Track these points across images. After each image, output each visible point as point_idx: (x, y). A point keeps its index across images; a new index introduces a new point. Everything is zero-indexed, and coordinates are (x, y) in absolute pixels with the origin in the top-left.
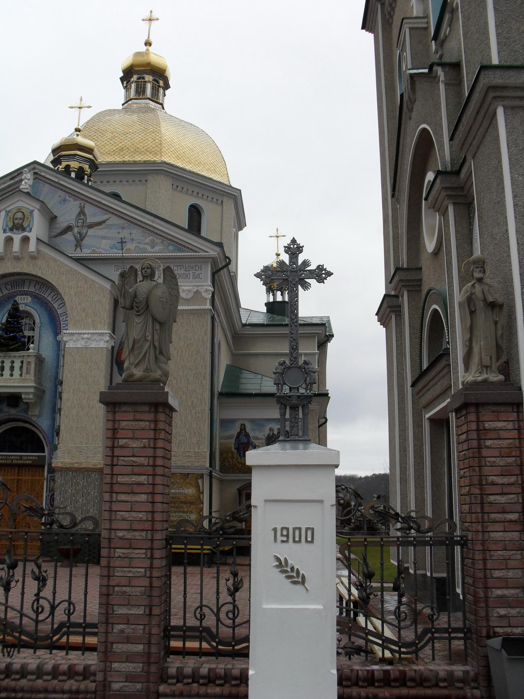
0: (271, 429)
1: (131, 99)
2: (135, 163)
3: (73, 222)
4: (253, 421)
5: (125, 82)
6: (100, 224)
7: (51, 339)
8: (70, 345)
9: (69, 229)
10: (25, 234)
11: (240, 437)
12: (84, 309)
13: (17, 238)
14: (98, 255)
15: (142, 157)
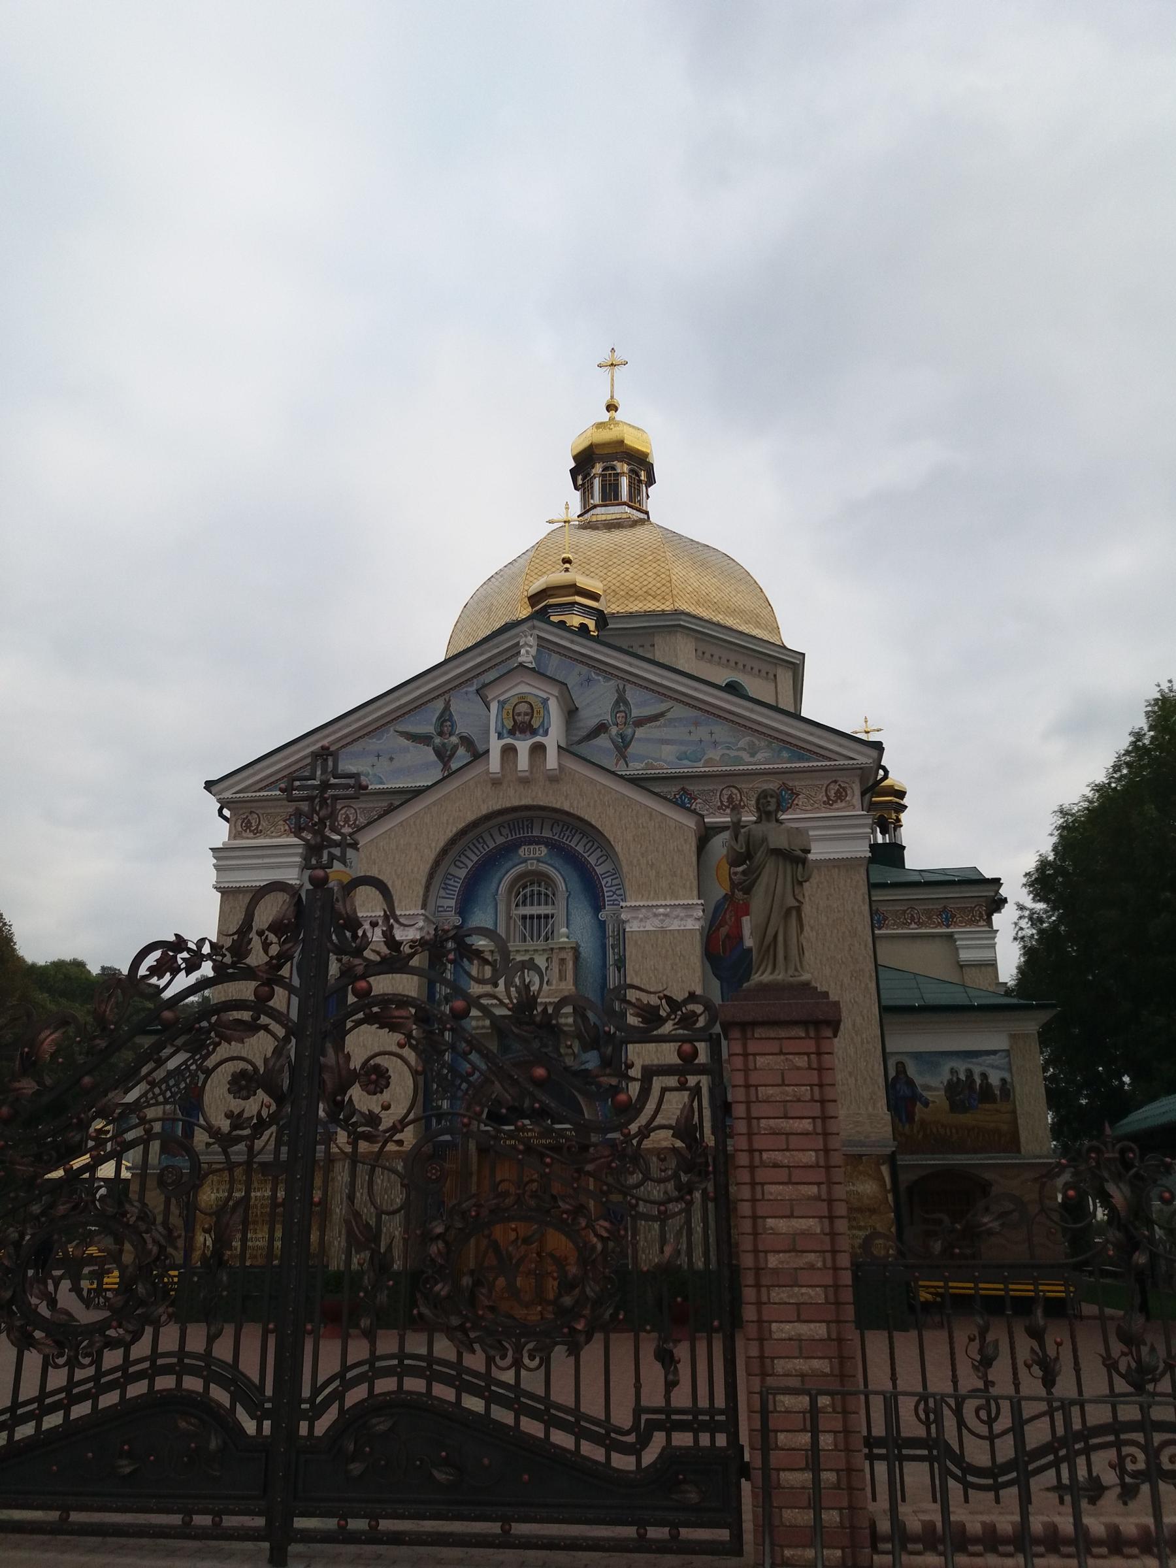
0: (953, 1071)
1: (595, 507)
2: (631, 616)
3: (608, 718)
4: (918, 1056)
5: (580, 477)
8: (633, 927)
9: (601, 728)
10: (538, 739)
11: (898, 1086)
12: (653, 864)
13: (523, 746)
14: (657, 771)
15: (640, 605)
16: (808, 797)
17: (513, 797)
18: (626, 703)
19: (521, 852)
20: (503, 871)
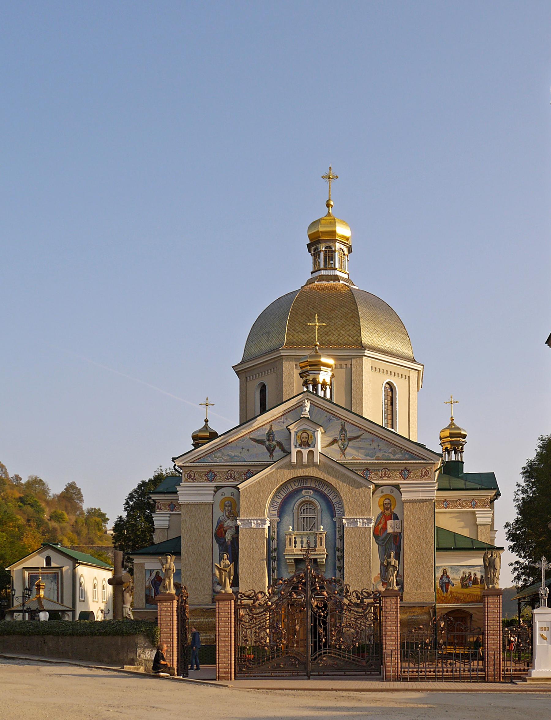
3: (337, 437)
4: (451, 567)
6: (356, 438)
7: (329, 520)
11: (443, 578)
16: (414, 474)
17: (301, 472)
18: (345, 431)
19: (303, 492)
20: (296, 500)
